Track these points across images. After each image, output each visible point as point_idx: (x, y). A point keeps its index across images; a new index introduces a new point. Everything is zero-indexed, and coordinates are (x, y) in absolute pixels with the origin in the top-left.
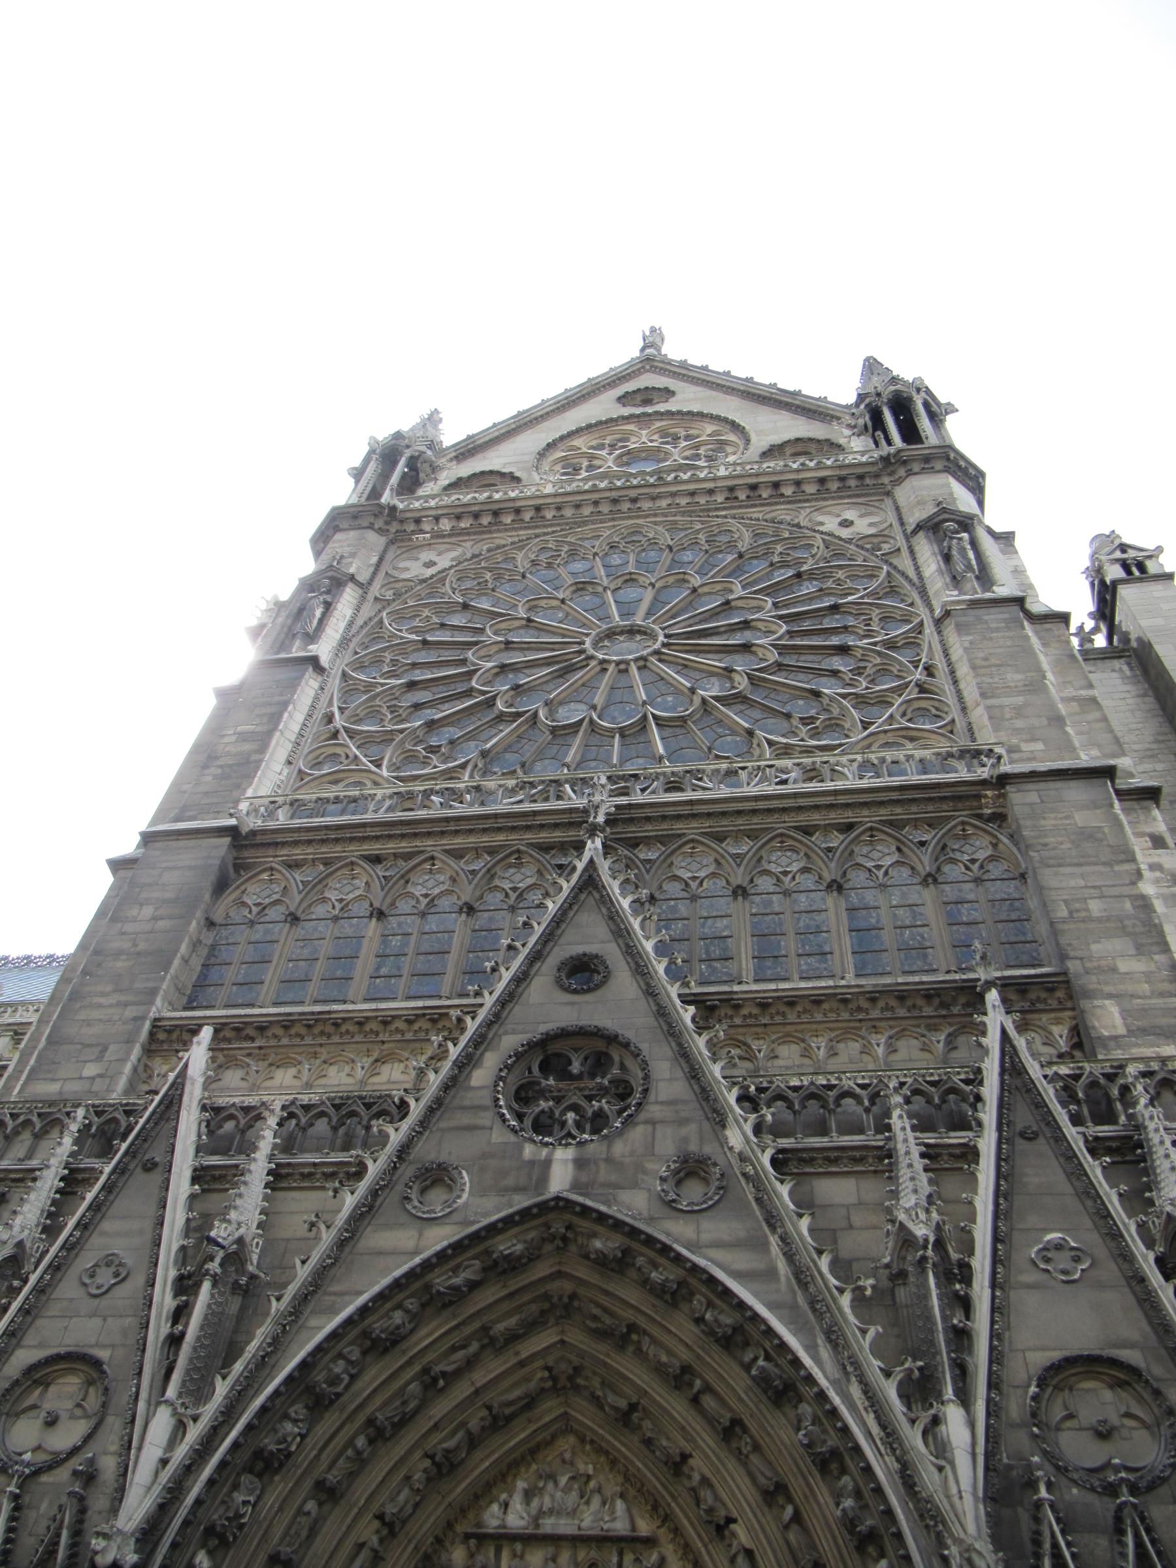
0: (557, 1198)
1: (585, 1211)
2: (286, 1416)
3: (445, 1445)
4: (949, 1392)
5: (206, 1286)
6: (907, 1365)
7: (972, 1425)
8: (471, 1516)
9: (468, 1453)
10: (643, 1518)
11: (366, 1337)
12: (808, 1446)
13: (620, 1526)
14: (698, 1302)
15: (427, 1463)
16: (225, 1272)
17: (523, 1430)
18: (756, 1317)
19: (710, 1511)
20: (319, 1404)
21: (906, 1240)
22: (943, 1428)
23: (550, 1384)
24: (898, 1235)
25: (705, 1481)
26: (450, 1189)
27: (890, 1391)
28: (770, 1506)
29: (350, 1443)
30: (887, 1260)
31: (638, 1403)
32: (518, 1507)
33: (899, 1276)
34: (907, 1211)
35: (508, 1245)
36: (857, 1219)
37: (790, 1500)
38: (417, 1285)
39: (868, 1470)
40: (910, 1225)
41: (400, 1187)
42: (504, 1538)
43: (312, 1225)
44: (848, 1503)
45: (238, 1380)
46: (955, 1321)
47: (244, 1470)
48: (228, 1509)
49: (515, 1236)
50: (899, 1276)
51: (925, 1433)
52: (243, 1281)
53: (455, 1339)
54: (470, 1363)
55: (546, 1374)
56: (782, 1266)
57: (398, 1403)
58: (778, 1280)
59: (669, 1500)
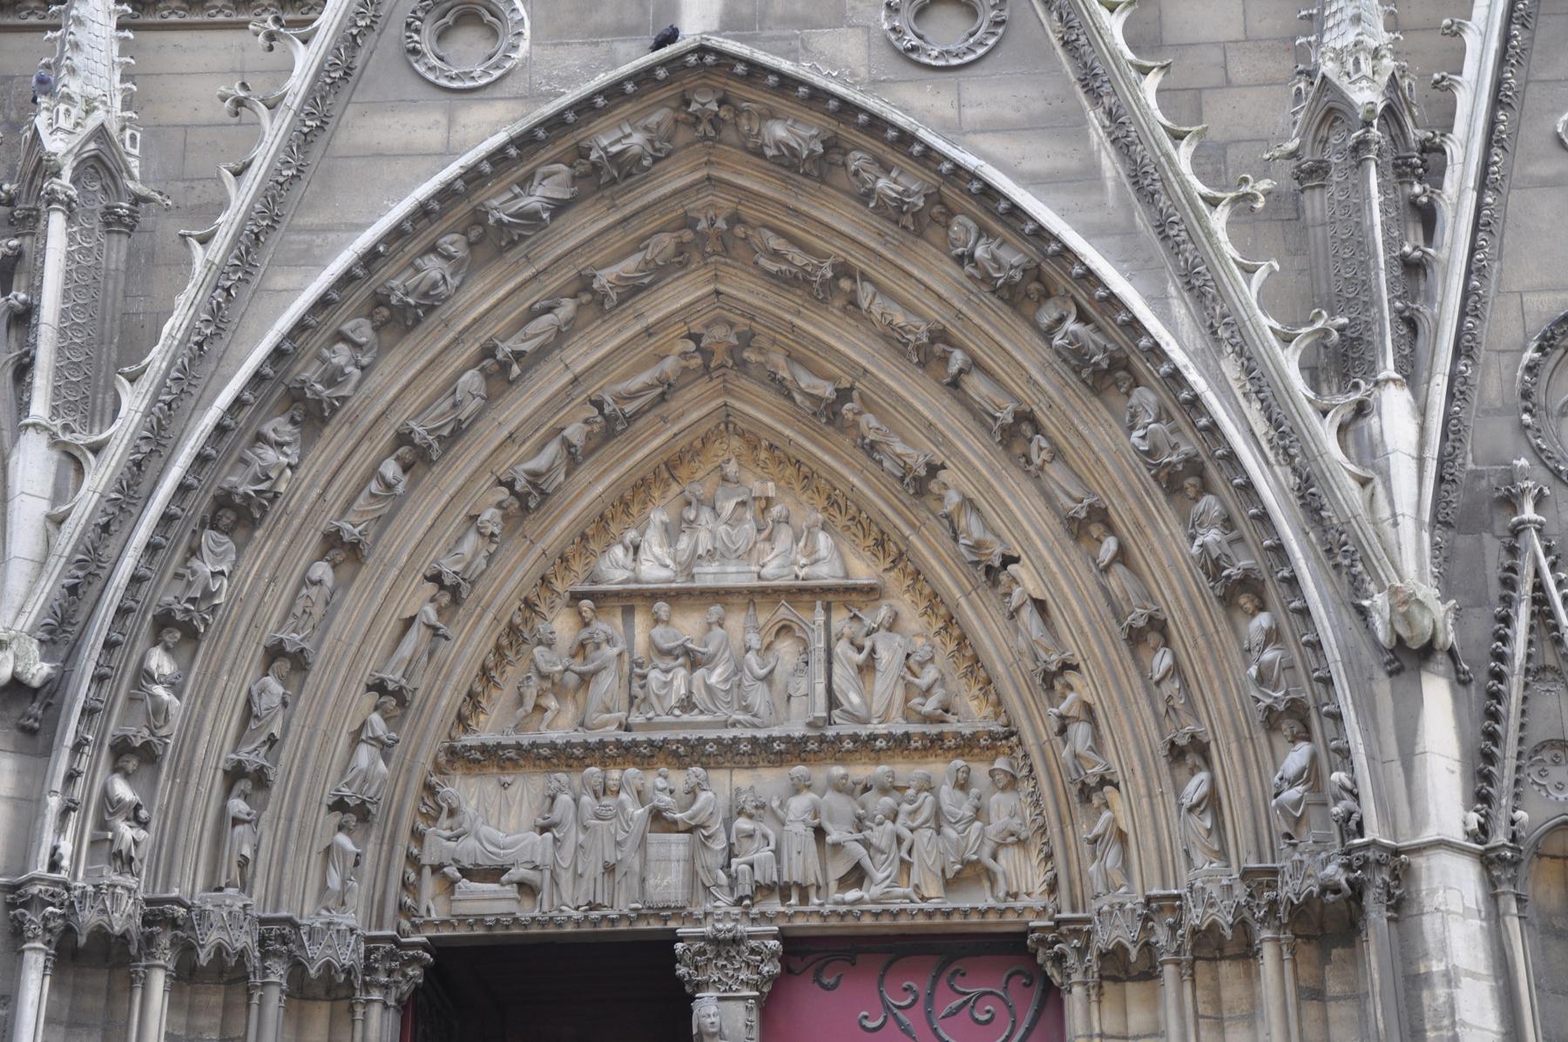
0: (702, 50)
1: (756, 71)
2: (260, 438)
3: (531, 465)
4: (1388, 369)
5: (56, 223)
6: (1319, 325)
7: (1422, 412)
8: (577, 566)
9: (567, 475)
10: (860, 557)
11: (379, 302)
12: (1148, 453)
13: (826, 572)
14: (961, 227)
15: (503, 494)
16: (83, 190)
17: (655, 434)
18: (1066, 254)
19: (977, 547)
20: (313, 416)
21: (1332, 110)
22: (1374, 421)
23: (697, 361)
24: (1316, 99)
25: (968, 503)
26: (494, 33)
27: (1289, 362)
28: (1077, 539)
29: (374, 472)
30: (1291, 146)
31: (852, 388)
32: (657, 550)
33: (1313, 174)
34: (1338, 55)
35: (617, 137)
36: (1239, 71)
37: (1110, 529)
38: (463, 209)
39: (1248, 487)
40: (1343, 83)
41: (395, 29)
42: (633, 599)
43: (239, 103)
44: (1212, 536)
45: (162, 384)
46: (1407, 249)
47: (203, 525)
48: (189, 584)
49: (627, 119)
50: (1313, 174)
51: (1342, 429)
52: (124, 207)
53: (535, 296)
54: (561, 336)
55: (691, 346)
56: (1110, 164)
57: (446, 405)
58: (1101, 188)
59: (907, 532)
